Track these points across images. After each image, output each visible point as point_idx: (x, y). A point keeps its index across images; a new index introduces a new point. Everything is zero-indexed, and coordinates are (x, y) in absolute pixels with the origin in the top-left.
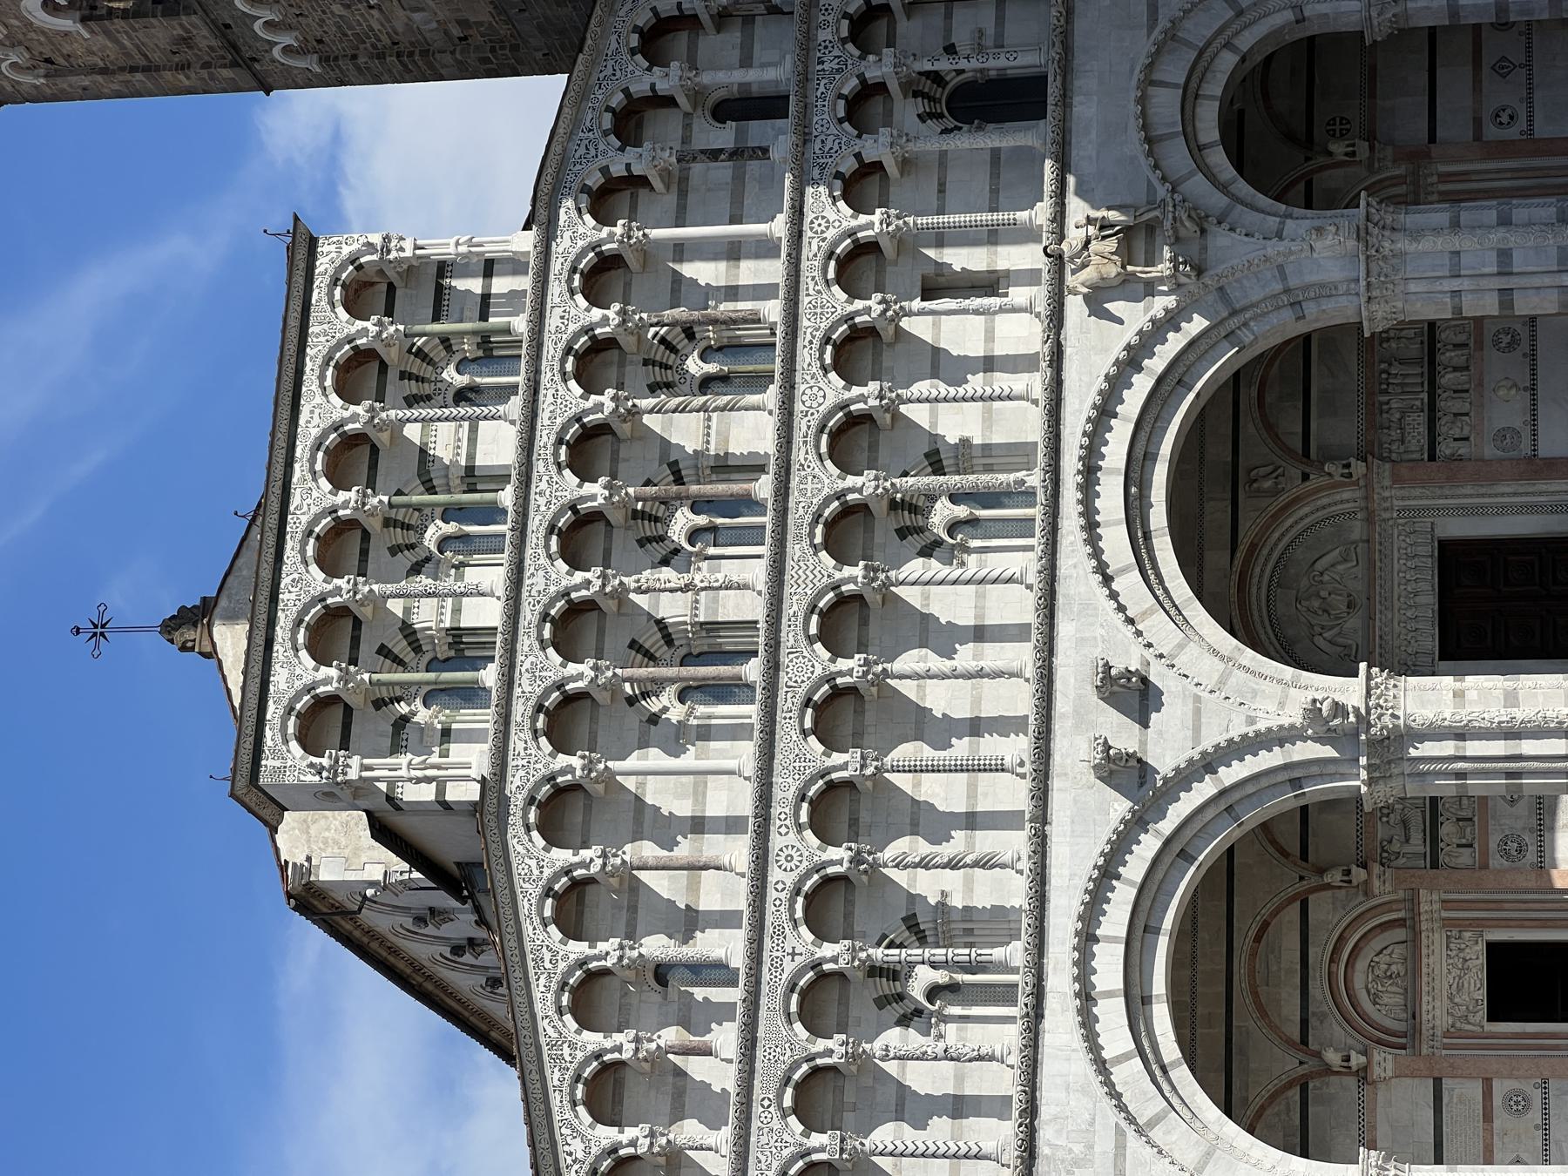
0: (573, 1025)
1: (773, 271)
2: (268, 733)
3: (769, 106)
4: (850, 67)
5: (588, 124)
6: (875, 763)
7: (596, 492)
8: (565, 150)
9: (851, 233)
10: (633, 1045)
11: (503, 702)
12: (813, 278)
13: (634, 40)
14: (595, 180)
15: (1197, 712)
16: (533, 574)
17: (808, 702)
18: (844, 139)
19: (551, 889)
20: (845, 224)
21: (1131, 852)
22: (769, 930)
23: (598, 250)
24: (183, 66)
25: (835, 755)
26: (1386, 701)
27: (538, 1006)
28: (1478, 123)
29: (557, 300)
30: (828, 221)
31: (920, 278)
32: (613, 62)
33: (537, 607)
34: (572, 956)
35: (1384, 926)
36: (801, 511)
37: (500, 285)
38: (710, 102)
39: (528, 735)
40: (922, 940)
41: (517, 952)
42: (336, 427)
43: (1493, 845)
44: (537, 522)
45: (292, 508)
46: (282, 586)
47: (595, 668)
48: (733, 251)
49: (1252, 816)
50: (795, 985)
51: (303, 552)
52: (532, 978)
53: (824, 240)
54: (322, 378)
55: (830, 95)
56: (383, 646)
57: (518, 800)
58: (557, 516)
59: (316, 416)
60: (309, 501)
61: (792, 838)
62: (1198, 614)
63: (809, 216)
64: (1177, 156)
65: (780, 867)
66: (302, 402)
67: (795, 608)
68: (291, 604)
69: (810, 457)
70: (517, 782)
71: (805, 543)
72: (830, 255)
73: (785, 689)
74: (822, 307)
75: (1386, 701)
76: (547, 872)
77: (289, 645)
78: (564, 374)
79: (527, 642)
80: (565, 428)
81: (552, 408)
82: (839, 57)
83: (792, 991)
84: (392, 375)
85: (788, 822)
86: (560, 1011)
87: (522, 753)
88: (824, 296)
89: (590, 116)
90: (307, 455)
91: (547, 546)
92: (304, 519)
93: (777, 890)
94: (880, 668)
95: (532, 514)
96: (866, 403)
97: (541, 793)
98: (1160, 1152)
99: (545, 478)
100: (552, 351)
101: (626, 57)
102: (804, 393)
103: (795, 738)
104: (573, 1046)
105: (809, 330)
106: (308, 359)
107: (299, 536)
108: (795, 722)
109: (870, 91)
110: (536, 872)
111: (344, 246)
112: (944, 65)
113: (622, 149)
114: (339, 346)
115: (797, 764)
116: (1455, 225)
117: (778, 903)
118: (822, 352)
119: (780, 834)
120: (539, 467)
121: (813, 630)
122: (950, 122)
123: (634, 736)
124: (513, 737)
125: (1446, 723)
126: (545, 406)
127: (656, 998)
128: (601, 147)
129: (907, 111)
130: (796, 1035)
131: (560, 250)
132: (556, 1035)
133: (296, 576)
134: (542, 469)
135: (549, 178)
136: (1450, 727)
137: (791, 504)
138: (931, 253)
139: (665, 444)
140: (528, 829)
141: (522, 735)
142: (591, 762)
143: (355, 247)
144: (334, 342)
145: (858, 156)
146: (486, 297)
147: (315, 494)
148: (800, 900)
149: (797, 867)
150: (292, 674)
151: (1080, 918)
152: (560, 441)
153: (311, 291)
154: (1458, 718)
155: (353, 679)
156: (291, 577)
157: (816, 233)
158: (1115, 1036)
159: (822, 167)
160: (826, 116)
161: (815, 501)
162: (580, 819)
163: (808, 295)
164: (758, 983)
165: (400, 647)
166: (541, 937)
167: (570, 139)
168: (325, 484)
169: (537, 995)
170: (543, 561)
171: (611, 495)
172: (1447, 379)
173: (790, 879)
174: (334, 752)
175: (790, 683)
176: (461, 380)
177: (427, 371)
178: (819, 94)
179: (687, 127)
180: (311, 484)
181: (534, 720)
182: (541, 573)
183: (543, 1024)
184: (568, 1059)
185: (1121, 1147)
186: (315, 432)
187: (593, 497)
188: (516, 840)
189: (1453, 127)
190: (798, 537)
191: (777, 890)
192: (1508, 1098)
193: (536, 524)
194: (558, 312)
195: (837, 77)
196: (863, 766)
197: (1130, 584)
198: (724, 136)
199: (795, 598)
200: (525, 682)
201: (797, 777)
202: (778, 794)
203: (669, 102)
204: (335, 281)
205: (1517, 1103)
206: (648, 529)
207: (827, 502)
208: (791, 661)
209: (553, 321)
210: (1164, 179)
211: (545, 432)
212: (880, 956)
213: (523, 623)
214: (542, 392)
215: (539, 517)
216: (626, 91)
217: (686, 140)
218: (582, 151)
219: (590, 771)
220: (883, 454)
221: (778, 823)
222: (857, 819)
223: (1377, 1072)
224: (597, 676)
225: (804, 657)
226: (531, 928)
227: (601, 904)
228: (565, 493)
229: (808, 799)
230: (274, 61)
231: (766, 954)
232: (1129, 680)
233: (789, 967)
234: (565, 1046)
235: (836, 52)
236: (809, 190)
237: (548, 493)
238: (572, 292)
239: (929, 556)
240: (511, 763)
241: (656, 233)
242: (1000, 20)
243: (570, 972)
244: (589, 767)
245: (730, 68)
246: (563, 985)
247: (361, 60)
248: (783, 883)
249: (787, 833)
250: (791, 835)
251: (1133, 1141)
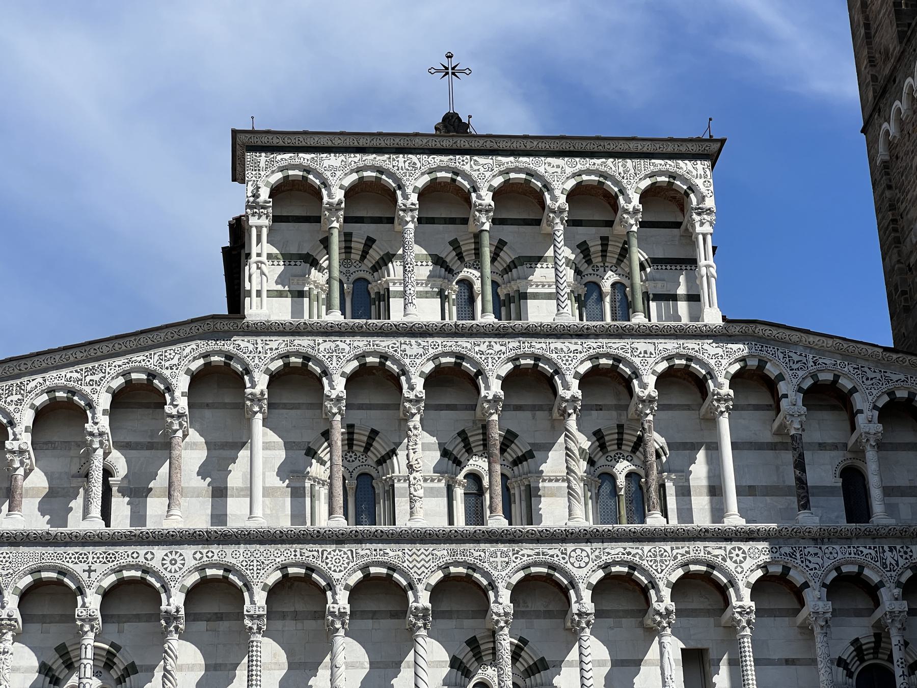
0: (38, 402)
1: (702, 518)
2: (287, 156)
4: (888, 574)
5: (820, 361)
6: (255, 627)
7: (494, 388)
8: (796, 344)
9: (732, 583)
10: (16, 449)
11: (309, 329)
12: (688, 552)
13: (902, 394)
14: (771, 370)
16: (420, 344)
17: (310, 569)
18: (819, 573)
19: (154, 377)
20: (740, 577)
22: (111, 550)
23: (708, 377)
24: (873, 61)
25: (264, 595)
27: (54, 374)
29: (661, 347)
30: (741, 562)
31: (705, 647)
32: (879, 377)
33: (391, 350)
34: (95, 397)
36: (476, 554)
37: (683, 307)
38: (859, 464)
39: (283, 349)
41: (99, 354)
42: (547, 186)
44: (465, 345)
45: (475, 158)
46: (410, 156)
47: (339, 399)
48: (716, 490)
50: (64, 574)
51: (440, 169)
52: (77, 368)
53: (724, 560)
54: (589, 172)
55: (860, 558)
56: (373, 241)
57: (228, 346)
58: (471, 360)
59: (555, 169)
60: (482, 170)
61: (191, 563)
63: (745, 546)
65: (166, 555)
66: (566, 159)
67: (391, 554)
68: (395, 163)
69: (525, 558)
70: (243, 344)
71: (449, 559)
72: (712, 566)
73: (320, 550)
74: (661, 561)
76: (167, 373)
77: (361, 164)
78: (597, 357)
79: (361, 344)
80: (549, 361)
81: (565, 349)
82: (897, 565)
83: (60, 573)
84: (604, 231)
85: (205, 559)
86: (50, 391)
87: (267, 347)
88: (672, 562)
89: (828, 362)
90: (521, 165)
91: (445, 354)
92: (467, 168)
93: (147, 553)
94: (338, 625)
95: (472, 340)
96: (576, 602)
97: (235, 365)
99: (504, 349)
101: (885, 388)
102: (582, 550)
103: (278, 560)
104: (19, 402)
105: (640, 552)
106: (604, 160)
107: (452, 165)
108: (292, 559)
109: (872, 591)
110: (167, 364)
111: (703, 180)
113: (800, 390)
114: (617, 183)
115: (255, 563)
117: (135, 555)
118: (621, 563)
119: (195, 553)
120: (513, 343)
121: (373, 570)
122: (856, 668)
123: (295, 437)
124: (281, 339)
126: (567, 344)
127: (75, 469)
128: (800, 373)
130: (21, 578)
131: (706, 346)
132: (29, 389)
133: (418, 165)
134: (511, 346)
135: (769, 332)
137: (482, 546)
138: (725, 657)
139: (549, 447)
140: (205, 356)
141: (283, 345)
142: (259, 400)
143: (703, 189)
144: (619, 178)
145: (806, 585)
146: (674, 298)
147: (488, 174)
148: (139, 574)
149: (166, 569)
150: (336, 169)
152: (537, 358)
153: (662, 159)
155: (332, 215)
156: (417, 162)
157: (730, 553)
159: (792, 555)
160: (840, 556)
161: (486, 565)
162: (227, 400)
163: (672, 549)
164: (66, 544)
165: (375, 254)
166: (112, 371)
167: (806, 347)
168: (498, 181)
169: (63, 372)
170: (432, 352)
171: (489, 401)
173: (156, 564)
174: (271, 204)
175: (325, 554)
176: (606, 286)
177: (612, 258)
178: (861, 549)
179: (835, 447)
180: (496, 170)
181: (297, 354)
182: (421, 351)
183: (39, 379)
184: (9, 400)
186: (541, 170)
187: (488, 387)
188: (195, 347)
190: (453, 553)
191: (147, 553)
194: (651, 348)
195: (878, 564)
196: (252, 617)
199: (400, 553)
200: (328, 345)
201: (244, 564)
202: (229, 549)
204: (673, 176)
206: (475, 439)
207: (486, 575)
208: (345, 553)
209: (642, 345)
211: (544, 346)
212: (86, 642)
213: (378, 340)
214: (579, 341)
215: (469, 345)
216: (854, 390)
217: (822, 446)
218: (796, 358)
219: (252, 400)
221: (204, 551)
222: (221, 619)
224: (332, 400)
225: (348, 564)
226: (120, 363)
228: (490, 365)
229: (226, 574)
230: (880, 126)
231: (91, 549)
233: (79, 569)
234: (20, 397)
235: (902, 562)
236: (765, 545)
237: (490, 351)
238: (669, 358)
239: (452, 666)
240: (259, 339)
241: (724, 423)
243: (84, 396)
244: (254, 399)
245: (881, 473)
246: (73, 392)
247: (888, 194)
248: (152, 559)
249: (195, 559)
250: (194, 562)
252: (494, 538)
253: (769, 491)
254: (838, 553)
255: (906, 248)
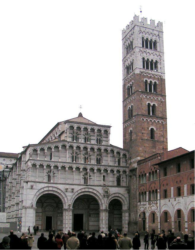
3: (119, 164)
15: (70, 196)
28: (115, 218)
35: (53, 209)
40: (53, 174)
43: (60, 217)
49: (62, 200)
61: (61, 165)
62: (78, 196)
64: (113, 196)
84: (99, 133)
100: (100, 147)
112: (121, 178)
116: (106, 216)
129: (118, 175)
158: (45, 189)
172: (95, 215)
185: (37, 189)
189: (115, 216)
192: (40, 218)
193: (87, 145)
197: (80, 191)
198: (117, 160)
203: (120, 156)
209: (103, 147)
210: (111, 195)
220: (91, 172)
223: (42, 208)
227: (57, 149)
233: (51, 164)
242: (125, 182)
251: (38, 190)
252: (88, 164)
253: (112, 161)
254: (117, 168)
255: (126, 137)
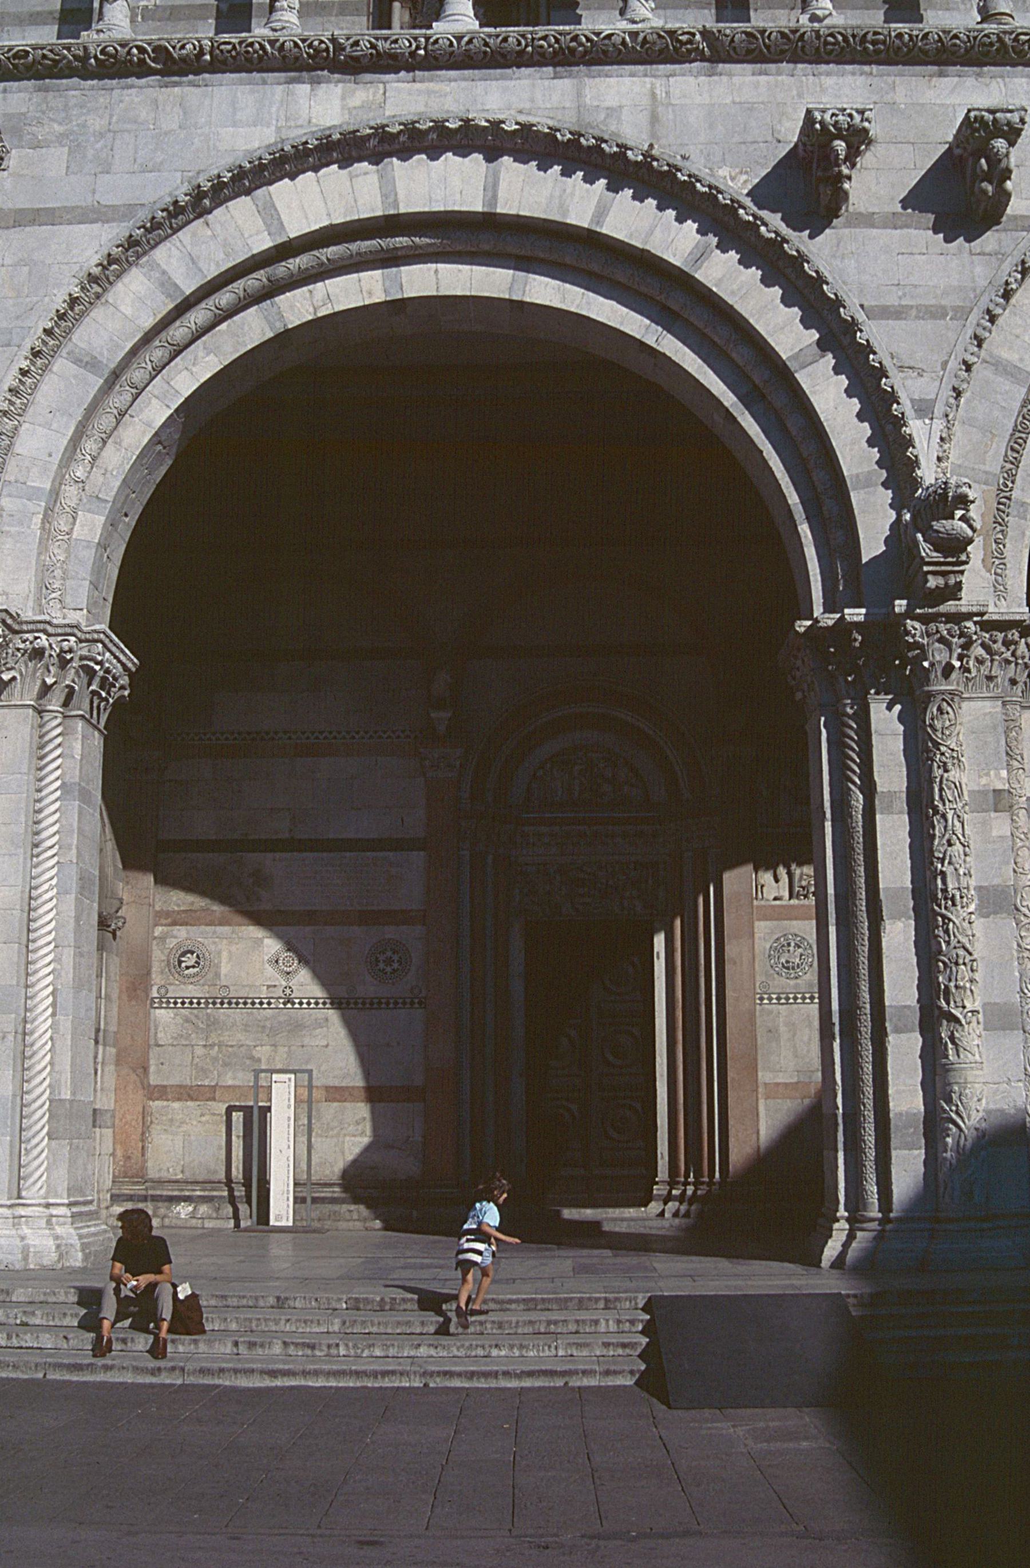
21: (661, 208)
26: (980, 661)
75: (980, 661)
98: (93, 279)
125: (937, 772)
136: (931, 781)
151: (526, 129)
154: (948, 794)
205: (389, 961)
232: (988, 177)
